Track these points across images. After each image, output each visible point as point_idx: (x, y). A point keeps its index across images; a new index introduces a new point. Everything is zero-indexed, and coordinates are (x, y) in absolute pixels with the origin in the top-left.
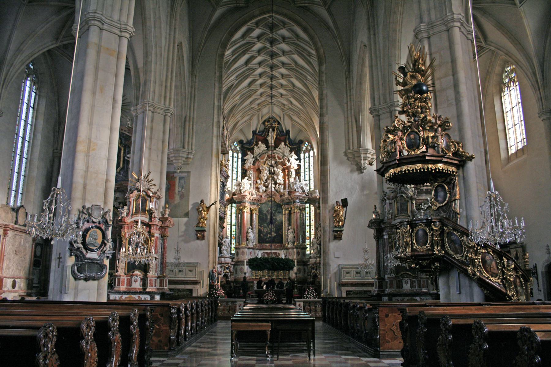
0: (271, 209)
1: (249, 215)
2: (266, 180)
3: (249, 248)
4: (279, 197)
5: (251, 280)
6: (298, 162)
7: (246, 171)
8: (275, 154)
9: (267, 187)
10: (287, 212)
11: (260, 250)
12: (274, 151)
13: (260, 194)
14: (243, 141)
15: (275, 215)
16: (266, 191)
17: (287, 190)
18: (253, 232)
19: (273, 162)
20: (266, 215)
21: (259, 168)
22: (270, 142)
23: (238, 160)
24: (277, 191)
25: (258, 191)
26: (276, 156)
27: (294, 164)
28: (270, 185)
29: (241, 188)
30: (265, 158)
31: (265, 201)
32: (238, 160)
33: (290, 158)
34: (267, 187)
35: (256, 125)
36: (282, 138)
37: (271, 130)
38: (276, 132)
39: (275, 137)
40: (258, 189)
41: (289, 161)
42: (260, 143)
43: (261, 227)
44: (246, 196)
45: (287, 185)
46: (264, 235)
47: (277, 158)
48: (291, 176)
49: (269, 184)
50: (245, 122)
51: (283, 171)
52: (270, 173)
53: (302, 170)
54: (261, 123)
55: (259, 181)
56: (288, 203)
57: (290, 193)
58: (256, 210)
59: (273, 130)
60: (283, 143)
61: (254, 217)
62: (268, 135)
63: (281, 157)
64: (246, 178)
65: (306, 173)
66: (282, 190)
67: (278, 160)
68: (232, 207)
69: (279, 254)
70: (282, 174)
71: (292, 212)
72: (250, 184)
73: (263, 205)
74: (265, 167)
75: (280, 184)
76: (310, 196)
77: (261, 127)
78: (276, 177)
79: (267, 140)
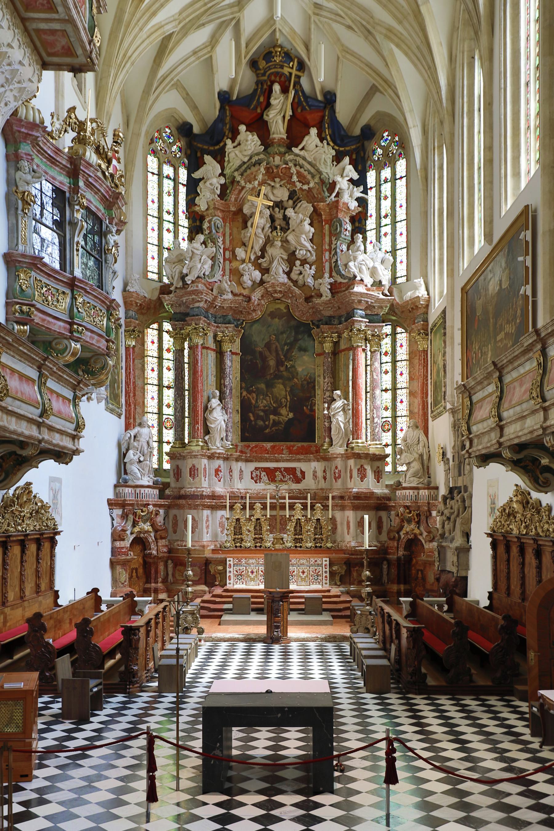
0: (277, 340)
1: (212, 356)
2: (263, 250)
3: (211, 457)
4: (302, 300)
5: (220, 556)
6: (358, 192)
7: (202, 218)
8: (291, 164)
9: (265, 271)
10: (328, 347)
11: (247, 461)
12: (288, 157)
13: (245, 292)
14: (191, 126)
15: (288, 357)
16: (262, 282)
17: (327, 280)
18: (225, 408)
19: (282, 194)
20: (264, 359)
21: (240, 210)
22: (273, 129)
23: (176, 189)
24: (295, 283)
25: (240, 284)
26: (293, 170)
27: (349, 199)
28: (275, 263)
29: (185, 271)
30: (260, 177)
31: (258, 314)
32: (176, 189)
33: (338, 179)
34: (265, 271)
35: (229, 70)
36: (311, 117)
37: (277, 88)
38: (292, 93)
39: (289, 113)
40: (237, 275)
41: (334, 184)
42: (242, 128)
43: (250, 392)
44: (197, 292)
45: (327, 265)
46: (258, 417)
47: (295, 178)
48: (337, 235)
49: (271, 262)
50: (195, 53)
51: (316, 218)
52: (273, 228)
53: (371, 224)
54: (244, 61)
55: (240, 253)
56: (329, 321)
57: (334, 288)
58: (232, 341)
59: (285, 90)
60: (314, 131)
61: (228, 363)
62: (268, 105)
63: (309, 177)
64: (201, 238)
65: (383, 230)
66: (310, 281)
67: (299, 185)
68: (160, 330)
69: (303, 473)
70: (313, 230)
71: (343, 346)
72: (213, 259)
73: (256, 327)
74: (261, 202)
75: (304, 262)
76: (396, 297)
77: (246, 81)
78: (291, 238)
79: (267, 122)
